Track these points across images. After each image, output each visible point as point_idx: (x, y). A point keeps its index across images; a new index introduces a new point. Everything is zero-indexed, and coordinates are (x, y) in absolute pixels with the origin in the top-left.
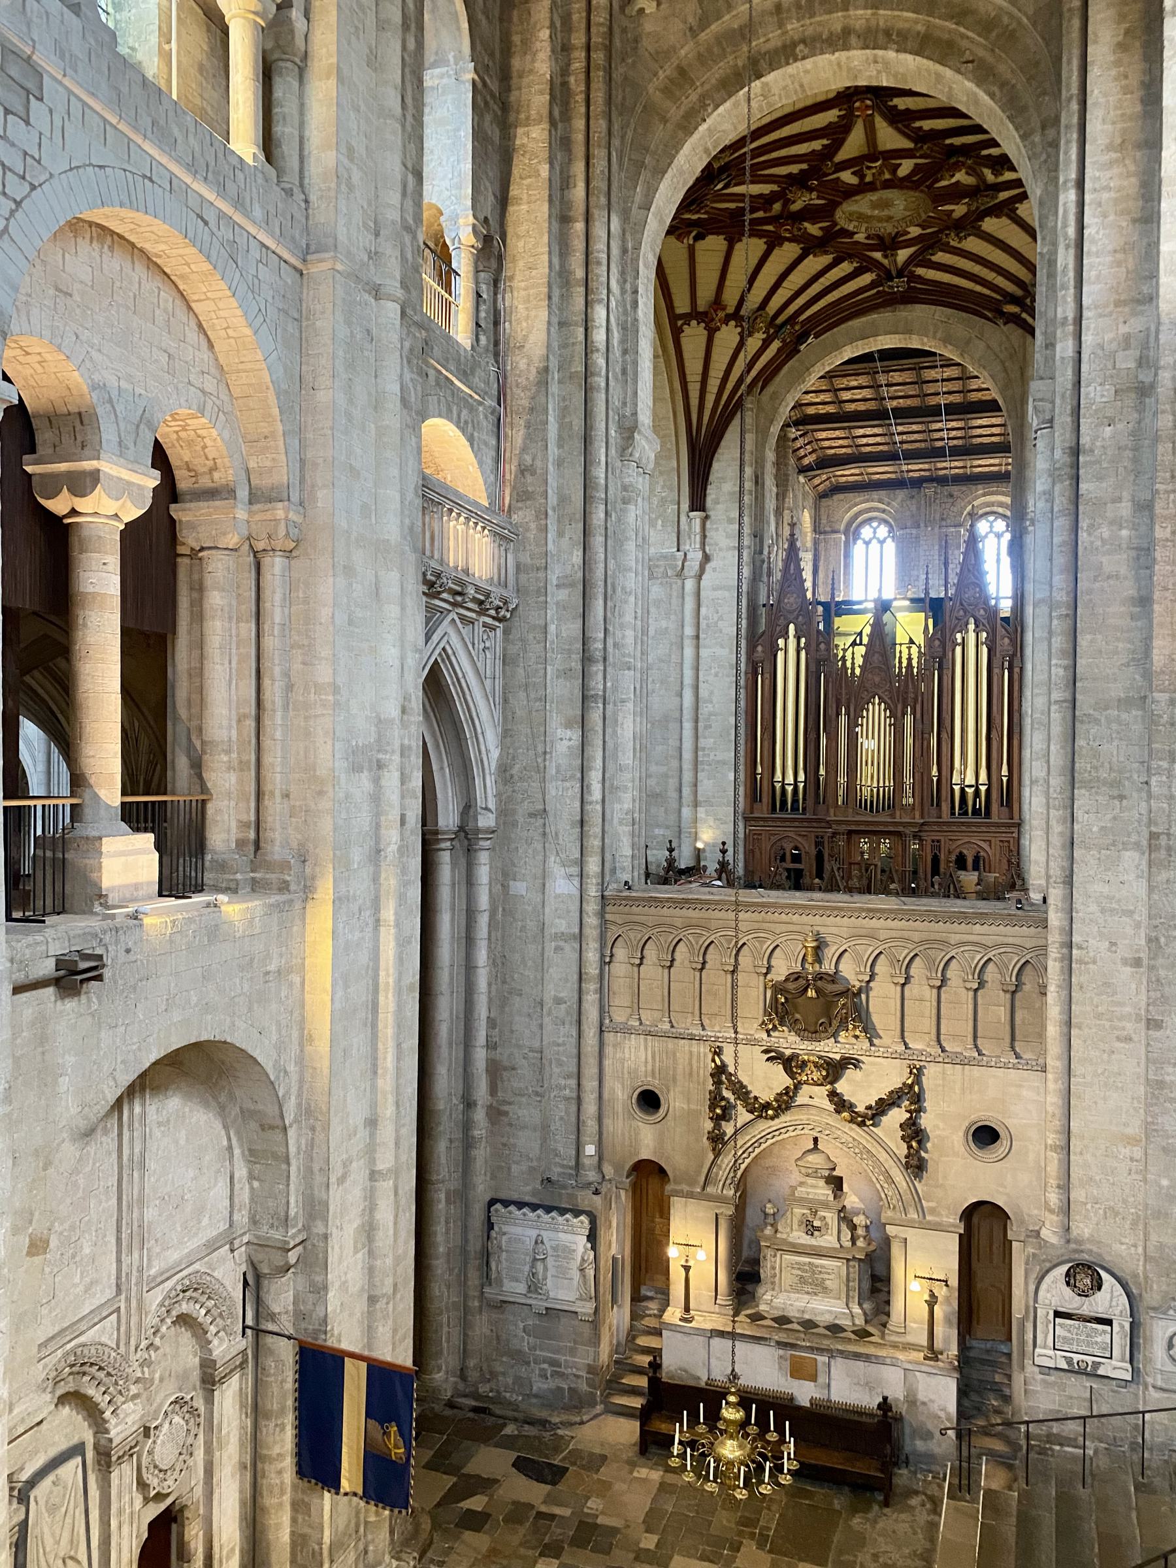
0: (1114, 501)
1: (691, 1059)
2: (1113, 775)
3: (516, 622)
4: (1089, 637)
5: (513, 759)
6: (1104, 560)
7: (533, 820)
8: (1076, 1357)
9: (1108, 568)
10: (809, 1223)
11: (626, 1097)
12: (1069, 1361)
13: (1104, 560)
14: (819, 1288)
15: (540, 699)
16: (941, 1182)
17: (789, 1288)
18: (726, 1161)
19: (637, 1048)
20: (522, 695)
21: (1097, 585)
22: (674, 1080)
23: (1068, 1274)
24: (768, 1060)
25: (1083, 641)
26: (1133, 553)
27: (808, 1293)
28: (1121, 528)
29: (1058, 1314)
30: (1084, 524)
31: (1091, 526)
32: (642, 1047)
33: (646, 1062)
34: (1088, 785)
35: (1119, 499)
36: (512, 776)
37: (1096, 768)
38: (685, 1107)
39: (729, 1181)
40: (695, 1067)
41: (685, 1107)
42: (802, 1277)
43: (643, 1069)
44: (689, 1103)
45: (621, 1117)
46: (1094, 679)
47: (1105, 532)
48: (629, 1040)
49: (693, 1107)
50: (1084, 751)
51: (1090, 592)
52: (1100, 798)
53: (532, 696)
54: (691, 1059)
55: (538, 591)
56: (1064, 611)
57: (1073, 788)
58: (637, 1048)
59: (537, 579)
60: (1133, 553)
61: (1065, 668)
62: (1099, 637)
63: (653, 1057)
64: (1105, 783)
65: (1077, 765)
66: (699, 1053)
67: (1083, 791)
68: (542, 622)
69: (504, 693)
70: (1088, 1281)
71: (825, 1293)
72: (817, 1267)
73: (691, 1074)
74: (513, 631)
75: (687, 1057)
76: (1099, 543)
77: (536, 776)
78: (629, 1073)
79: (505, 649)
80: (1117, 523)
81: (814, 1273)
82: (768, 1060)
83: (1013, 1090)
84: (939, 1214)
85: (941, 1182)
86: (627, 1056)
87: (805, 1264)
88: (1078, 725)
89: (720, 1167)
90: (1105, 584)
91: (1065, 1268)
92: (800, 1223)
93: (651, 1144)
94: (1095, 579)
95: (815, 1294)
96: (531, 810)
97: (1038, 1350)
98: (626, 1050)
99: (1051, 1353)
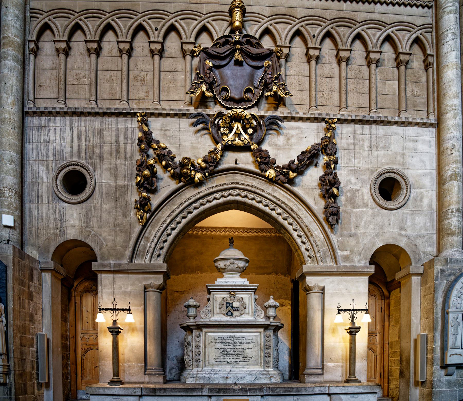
1: (118, 136)
10: (229, 305)
11: (50, 180)
16: (353, 231)
17: (212, 361)
18: (154, 233)
19: (63, 130)
22: (101, 158)
24: (199, 131)
27: (230, 363)
32: (68, 129)
33: (72, 142)
38: (112, 183)
39: (156, 253)
40: (122, 146)
41: (112, 183)
42: (224, 350)
43: (68, 149)
44: (116, 180)
45: (45, 200)
48: (54, 122)
49: (120, 182)
54: (118, 136)
58: (63, 130)
63: (79, 138)
66: (126, 129)
71: (246, 361)
72: (237, 339)
73: (118, 151)
75: (114, 134)
78: (54, 155)
81: (235, 345)
82: (199, 131)
83: (411, 145)
84: (352, 261)
85: (353, 231)
86: (52, 138)
87: (227, 338)
89: (148, 239)
92: (221, 306)
93: (77, 223)
95: (237, 363)
98: (51, 133)
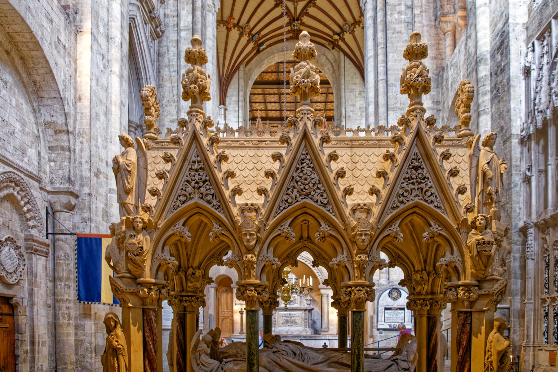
0: (399, 5)
2: (402, 105)
3: (164, 38)
4: (392, 55)
5: (163, 97)
6: (396, 26)
7: (172, 124)
8: (392, 324)
9: (398, 30)
12: (390, 325)
13: (396, 26)
14: (295, 323)
15: (175, 71)
20: (167, 69)
21: (394, 35)
23: (389, 293)
25: (390, 56)
26: (406, 24)
28: (401, 15)
29: (386, 309)
30: (389, 13)
31: (391, 14)
34: (393, 109)
35: (400, 4)
36: (162, 105)
37: (396, 103)
46: (394, 70)
47: (396, 16)
50: (391, 97)
51: (391, 38)
52: (397, 114)
53: (171, 70)
55: (174, 25)
56: (382, 46)
57: (387, 111)
59: (174, 21)
60: (406, 24)
61: (384, 67)
62: (395, 54)
64: (399, 109)
65: (389, 103)
67: (391, 112)
68: (176, 38)
69: (159, 69)
70: (396, 294)
74: (163, 42)
76: (394, 20)
77: (173, 105)
79: (159, 50)
80: (400, 13)
88: (389, 87)
90: (397, 35)
91: (388, 291)
94: (393, 33)
96: (171, 119)
97: (379, 323)
99: (384, 323)
